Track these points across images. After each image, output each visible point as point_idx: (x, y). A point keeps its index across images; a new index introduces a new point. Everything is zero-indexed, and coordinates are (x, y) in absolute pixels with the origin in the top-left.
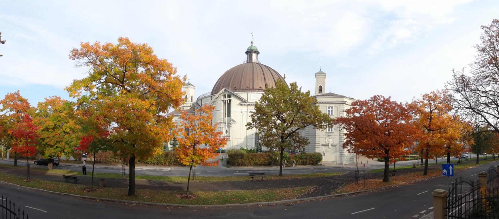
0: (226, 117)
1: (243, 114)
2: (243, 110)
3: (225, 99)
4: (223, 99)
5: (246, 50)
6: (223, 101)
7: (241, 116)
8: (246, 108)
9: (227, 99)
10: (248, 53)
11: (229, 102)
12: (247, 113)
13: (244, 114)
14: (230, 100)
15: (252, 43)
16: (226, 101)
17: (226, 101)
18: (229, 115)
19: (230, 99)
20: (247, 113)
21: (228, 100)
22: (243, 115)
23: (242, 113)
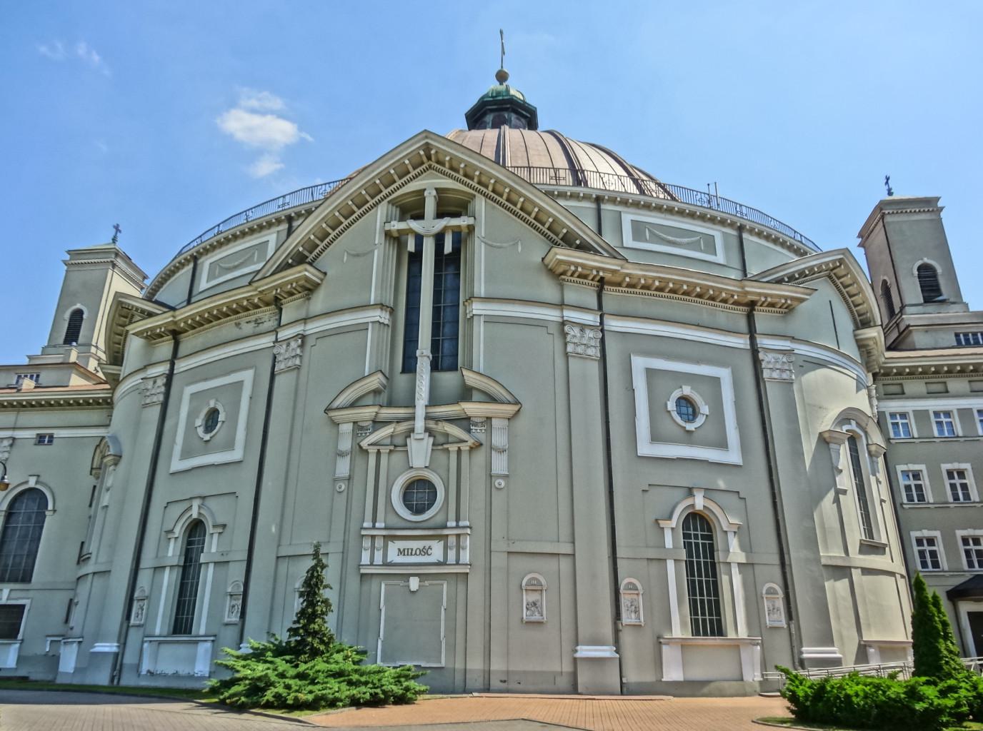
0: (423, 365)
1: (570, 348)
2: (570, 315)
3: (414, 225)
4: (396, 226)
5: (472, 102)
6: (396, 240)
7: (560, 362)
8: (595, 306)
9: (430, 225)
10: (484, 114)
11: (448, 248)
12: (603, 341)
13: (580, 350)
14: (461, 238)
15: (502, 77)
16: (419, 239)
17: (419, 239)
18: (444, 360)
19: (463, 222)
20: (603, 341)
21: (439, 238)
22: (579, 356)
23: (564, 335)
